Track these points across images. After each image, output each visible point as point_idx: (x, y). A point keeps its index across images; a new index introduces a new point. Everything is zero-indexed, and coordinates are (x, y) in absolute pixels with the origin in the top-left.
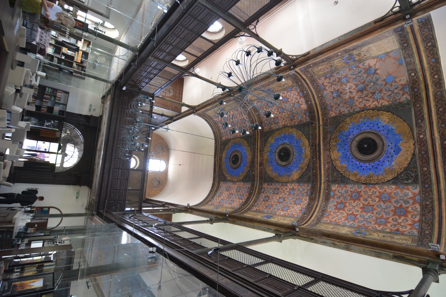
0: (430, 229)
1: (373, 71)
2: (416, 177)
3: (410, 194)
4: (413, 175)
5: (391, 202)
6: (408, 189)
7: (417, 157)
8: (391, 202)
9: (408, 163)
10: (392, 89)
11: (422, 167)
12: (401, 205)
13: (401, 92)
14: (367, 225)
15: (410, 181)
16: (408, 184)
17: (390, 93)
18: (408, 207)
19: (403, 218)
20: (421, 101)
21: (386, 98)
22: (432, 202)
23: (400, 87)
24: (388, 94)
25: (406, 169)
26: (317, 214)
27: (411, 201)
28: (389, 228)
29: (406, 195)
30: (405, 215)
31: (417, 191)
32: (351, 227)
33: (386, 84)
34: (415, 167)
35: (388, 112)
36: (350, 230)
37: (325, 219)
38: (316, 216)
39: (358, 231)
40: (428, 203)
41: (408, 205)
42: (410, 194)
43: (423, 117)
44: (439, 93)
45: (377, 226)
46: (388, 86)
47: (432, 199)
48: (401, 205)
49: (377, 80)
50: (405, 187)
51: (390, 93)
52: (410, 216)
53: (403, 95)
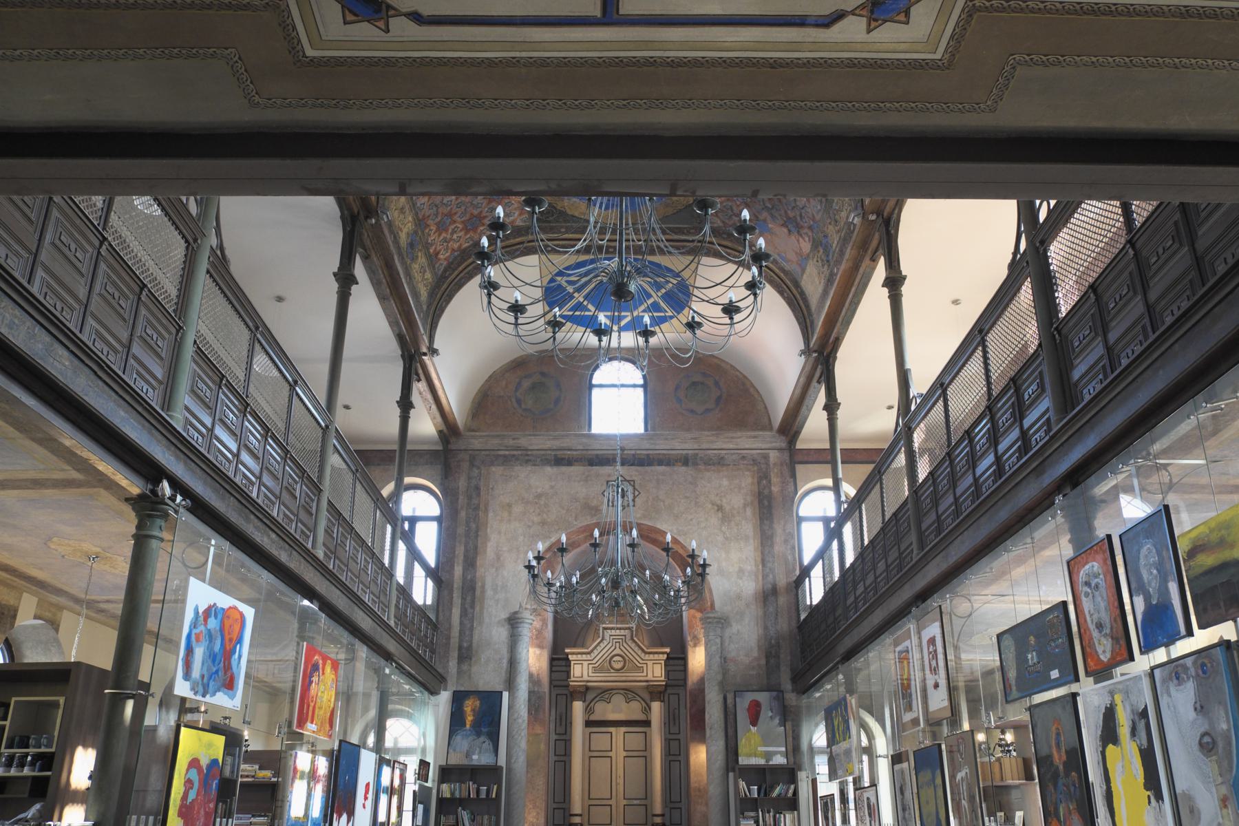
11: (567, 228)
13: (731, 223)
19: (462, 234)
34: (565, 221)
49: (773, 217)
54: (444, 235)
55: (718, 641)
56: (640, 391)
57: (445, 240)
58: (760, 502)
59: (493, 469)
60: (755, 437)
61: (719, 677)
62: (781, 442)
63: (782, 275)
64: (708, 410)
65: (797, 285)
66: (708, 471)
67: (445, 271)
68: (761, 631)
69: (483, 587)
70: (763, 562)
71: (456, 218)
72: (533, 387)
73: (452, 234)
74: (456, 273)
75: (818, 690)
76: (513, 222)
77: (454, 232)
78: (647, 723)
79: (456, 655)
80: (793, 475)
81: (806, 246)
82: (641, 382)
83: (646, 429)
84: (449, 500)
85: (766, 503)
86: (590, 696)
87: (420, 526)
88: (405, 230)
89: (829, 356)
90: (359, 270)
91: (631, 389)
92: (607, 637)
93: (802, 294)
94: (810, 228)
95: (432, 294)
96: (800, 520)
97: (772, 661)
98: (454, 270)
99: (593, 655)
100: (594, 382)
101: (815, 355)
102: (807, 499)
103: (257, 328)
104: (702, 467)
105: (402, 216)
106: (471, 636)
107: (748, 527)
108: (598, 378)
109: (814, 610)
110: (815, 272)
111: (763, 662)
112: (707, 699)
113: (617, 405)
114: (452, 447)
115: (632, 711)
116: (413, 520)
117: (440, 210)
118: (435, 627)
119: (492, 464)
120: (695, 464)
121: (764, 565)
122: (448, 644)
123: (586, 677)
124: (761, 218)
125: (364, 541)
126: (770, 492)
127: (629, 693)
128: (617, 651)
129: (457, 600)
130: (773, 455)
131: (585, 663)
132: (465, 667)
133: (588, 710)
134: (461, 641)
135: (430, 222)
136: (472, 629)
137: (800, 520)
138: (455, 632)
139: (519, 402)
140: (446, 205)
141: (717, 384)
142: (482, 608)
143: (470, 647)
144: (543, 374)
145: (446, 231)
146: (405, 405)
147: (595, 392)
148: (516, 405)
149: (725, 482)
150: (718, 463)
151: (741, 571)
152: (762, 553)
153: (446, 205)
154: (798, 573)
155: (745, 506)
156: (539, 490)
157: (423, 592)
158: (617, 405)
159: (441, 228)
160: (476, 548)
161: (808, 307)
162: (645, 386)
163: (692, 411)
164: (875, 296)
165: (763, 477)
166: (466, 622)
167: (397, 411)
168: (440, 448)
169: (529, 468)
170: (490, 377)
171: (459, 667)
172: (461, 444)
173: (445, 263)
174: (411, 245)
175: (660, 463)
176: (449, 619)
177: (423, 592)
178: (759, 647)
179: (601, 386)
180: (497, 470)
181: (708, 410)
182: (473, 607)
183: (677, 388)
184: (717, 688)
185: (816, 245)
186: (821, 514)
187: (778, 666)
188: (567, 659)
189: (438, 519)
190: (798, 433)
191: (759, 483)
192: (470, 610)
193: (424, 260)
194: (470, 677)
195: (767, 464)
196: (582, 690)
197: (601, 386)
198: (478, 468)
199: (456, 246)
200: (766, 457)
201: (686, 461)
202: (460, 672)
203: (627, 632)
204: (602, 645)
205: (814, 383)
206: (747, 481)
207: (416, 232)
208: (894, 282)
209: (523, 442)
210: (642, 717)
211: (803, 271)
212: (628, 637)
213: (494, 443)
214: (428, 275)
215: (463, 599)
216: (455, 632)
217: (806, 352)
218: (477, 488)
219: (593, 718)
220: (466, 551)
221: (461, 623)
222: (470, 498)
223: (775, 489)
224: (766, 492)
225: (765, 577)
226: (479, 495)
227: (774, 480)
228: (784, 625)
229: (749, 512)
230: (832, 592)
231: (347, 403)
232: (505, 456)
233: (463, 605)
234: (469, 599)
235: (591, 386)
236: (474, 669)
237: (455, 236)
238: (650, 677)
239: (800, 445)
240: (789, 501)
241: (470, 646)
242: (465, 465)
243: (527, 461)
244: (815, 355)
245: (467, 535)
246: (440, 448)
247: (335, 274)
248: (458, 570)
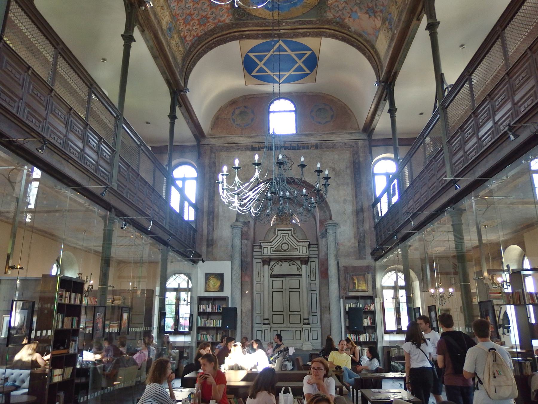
1: (370, 13)
2: (243, 20)
3: (223, 18)
4: (244, 18)
5: (211, 9)
6: (228, 16)
7: (262, 21)
8: (211, 9)
9: (257, 15)
10: (344, 11)
12: (209, 17)
13: (338, 15)
15: (237, 16)
16: (233, 15)
17: (341, 8)
18: (209, 22)
19: (198, 27)
20: (322, 24)
21: (337, 3)
22: (219, 32)
23: (343, 17)
24: (340, 6)
25: (249, 14)
27: (216, 21)
29: (222, 16)
30: (201, 26)
31: (227, 21)
33: (352, 10)
34: (251, 19)
35: (319, 3)
40: (217, 31)
41: (212, 21)
42: (223, 18)
43: (305, 24)
44: (325, 34)
46: (349, 10)
47: (223, 31)
48: (209, 17)
49: (360, 8)
50: (230, 14)
51: (341, 8)
52: (201, 28)
53: (334, 15)
54: (188, 27)
55: (334, 234)
56: (293, 115)
57: (189, 30)
58: (354, 166)
59: (222, 153)
60: (351, 134)
61: (335, 253)
62: (364, 136)
63: (365, 43)
64: (327, 122)
65: (373, 47)
66: (328, 151)
67: (190, 47)
68: (355, 230)
70: (356, 196)
71: (194, 16)
72: (241, 113)
73: (192, 27)
74: (197, 49)
75: (386, 258)
76: (224, 20)
77: (193, 25)
78: (300, 275)
79: (206, 244)
80: (371, 152)
81: (378, 23)
82: (294, 109)
83: (296, 132)
84: (201, 169)
85: (357, 166)
86: (272, 263)
87: (187, 182)
88: (165, 20)
89: (391, 83)
90: (137, 33)
91: (289, 113)
92: (279, 234)
93: (376, 52)
94: (381, 11)
95: (184, 60)
96: (374, 175)
97: (361, 244)
98: (196, 48)
99: (273, 243)
100: (270, 110)
101: (383, 84)
102: (378, 164)
103: (58, 44)
104: (325, 149)
105: (162, 11)
107: (348, 179)
108: (272, 108)
109: (382, 218)
110: (384, 37)
111: (357, 245)
112: (329, 263)
113: (283, 120)
114: (202, 143)
115: (293, 269)
116: (184, 180)
117: (185, 11)
118: (195, 230)
119: (221, 151)
120: (321, 148)
121: (356, 197)
123: (269, 254)
124: (354, 10)
125: (146, 183)
126: (359, 161)
127: (290, 260)
128: (286, 242)
129: (206, 218)
130: (360, 143)
131: (269, 247)
132: (210, 250)
133: (272, 269)
135: (179, 18)
137: (374, 175)
138: (205, 232)
139: (234, 120)
140: (188, 9)
141: (331, 109)
142: (218, 221)
143: (212, 240)
144: (245, 107)
145: (189, 24)
146: (173, 117)
147: (271, 115)
148: (232, 122)
149: (336, 157)
150: (333, 147)
151: (345, 200)
152: (356, 192)
153: (188, 9)
154: (373, 201)
155: (347, 168)
156: (244, 163)
157: (190, 215)
158: (283, 120)
159: (186, 23)
160: (214, 192)
161: (379, 59)
162: (295, 111)
163: (319, 123)
164: (422, 34)
165: (355, 153)
166: (210, 228)
167: (168, 120)
168: (196, 144)
169: (239, 152)
170: (220, 109)
172: (204, 142)
173: (190, 43)
174: (170, 29)
175: (304, 148)
176: (202, 227)
177: (190, 215)
178: (355, 237)
179: (274, 112)
180: (224, 154)
181: (327, 122)
182: (213, 220)
183: (312, 111)
184: (334, 258)
185: (384, 21)
186: (385, 172)
187: (364, 247)
188: (261, 246)
189: (196, 179)
190: (373, 130)
191: (353, 157)
192: (212, 222)
193: (178, 39)
194: (213, 254)
195: (357, 147)
196: (268, 260)
197: (274, 112)
198: (215, 153)
199: (195, 34)
200: (357, 144)
201: (316, 147)
202: (208, 252)
203: (289, 232)
204: (277, 238)
205: (382, 101)
206: (347, 156)
207: (171, 22)
208: (432, 27)
209: (236, 140)
210: (298, 273)
211: (377, 38)
212: (290, 234)
213: (222, 140)
214: (181, 49)
215: (209, 217)
216: (205, 232)
217: (379, 82)
218: (214, 163)
219: (273, 273)
220: (210, 194)
221: (208, 228)
222: (211, 168)
223: (361, 159)
224: (357, 161)
225: (357, 203)
226: (215, 166)
227: (361, 155)
228: (368, 226)
229: (349, 171)
230: (392, 208)
231: (148, 121)
232: (227, 147)
233: (208, 219)
234: (211, 217)
235: (269, 112)
237: (194, 28)
238: (301, 253)
239: (374, 137)
240: (368, 166)
242: (208, 152)
243: (238, 149)
244: (383, 84)
246: (196, 144)
247: (122, 36)
248: (206, 203)
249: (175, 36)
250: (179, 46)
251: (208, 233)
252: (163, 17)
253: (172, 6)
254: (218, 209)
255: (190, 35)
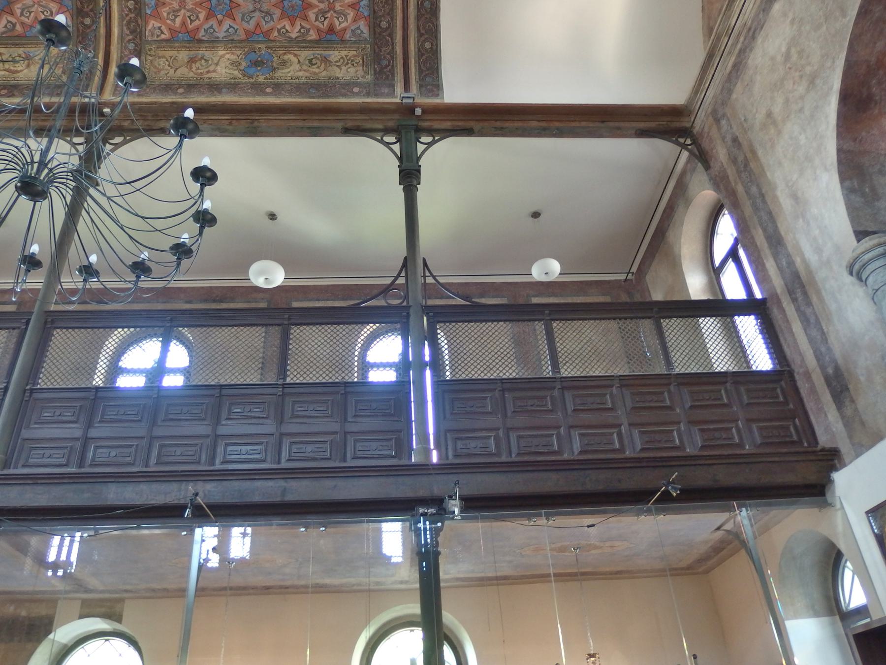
0: (388, 14)
14: (266, 27)
26: (121, 11)
28: (314, 26)
32: (230, 43)
36: (234, 57)
37: (153, 24)
38: (121, 19)
39: (254, 57)
45: (287, 24)
67: (374, 26)
69: (804, 260)
106: (829, 349)
122: (813, 390)
132: (848, 411)
134: (823, 368)
136: (825, 340)
160: (770, 213)
171: (843, 417)
182: (809, 303)
192: (808, 311)
193: (305, 54)
215: (794, 300)
220: (765, 230)
221: (811, 341)
233: (798, 309)
236: (861, 403)
241: (837, 369)
245: (756, 209)
249: (286, 57)
250: (325, 60)
251: (818, 356)
252: (211, 68)
253: (221, 35)
254: (801, 254)
255: (340, 13)
